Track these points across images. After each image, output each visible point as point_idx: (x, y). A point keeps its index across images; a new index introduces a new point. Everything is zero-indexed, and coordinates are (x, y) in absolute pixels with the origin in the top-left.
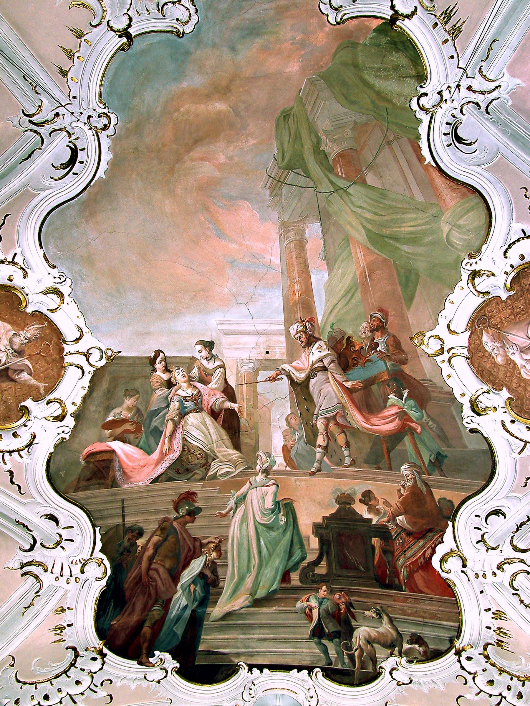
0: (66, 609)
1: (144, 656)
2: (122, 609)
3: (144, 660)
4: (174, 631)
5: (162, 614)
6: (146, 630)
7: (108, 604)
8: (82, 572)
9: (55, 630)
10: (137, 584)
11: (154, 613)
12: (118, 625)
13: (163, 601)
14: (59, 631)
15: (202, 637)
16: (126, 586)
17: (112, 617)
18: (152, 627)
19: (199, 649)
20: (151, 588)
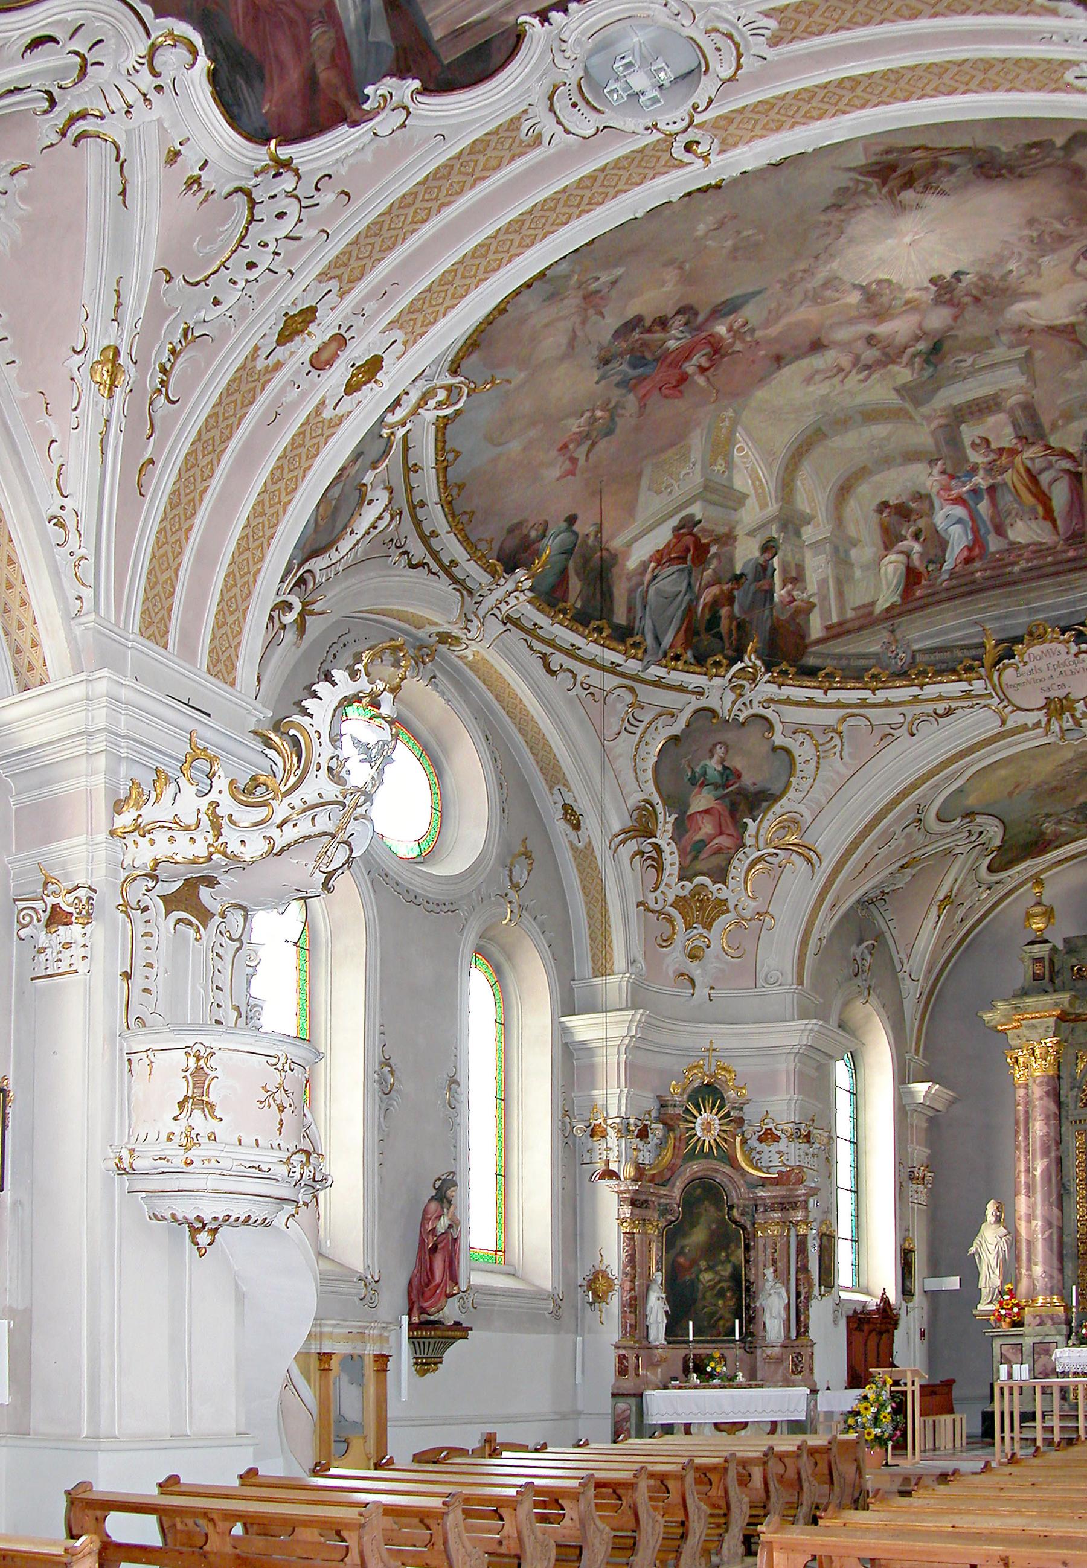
0: (180, 147)
1: (352, 110)
2: (262, 79)
3: (356, 115)
4: (374, 43)
5: (332, 35)
6: (325, 75)
7: (232, 86)
8: (156, 75)
9: (189, 187)
10: (256, 19)
11: (319, 43)
12: (276, 106)
13: (320, 12)
14: (195, 187)
15: (428, 18)
16: (242, 37)
17: (258, 102)
18: (333, 64)
19: (436, 39)
20: (284, 7)
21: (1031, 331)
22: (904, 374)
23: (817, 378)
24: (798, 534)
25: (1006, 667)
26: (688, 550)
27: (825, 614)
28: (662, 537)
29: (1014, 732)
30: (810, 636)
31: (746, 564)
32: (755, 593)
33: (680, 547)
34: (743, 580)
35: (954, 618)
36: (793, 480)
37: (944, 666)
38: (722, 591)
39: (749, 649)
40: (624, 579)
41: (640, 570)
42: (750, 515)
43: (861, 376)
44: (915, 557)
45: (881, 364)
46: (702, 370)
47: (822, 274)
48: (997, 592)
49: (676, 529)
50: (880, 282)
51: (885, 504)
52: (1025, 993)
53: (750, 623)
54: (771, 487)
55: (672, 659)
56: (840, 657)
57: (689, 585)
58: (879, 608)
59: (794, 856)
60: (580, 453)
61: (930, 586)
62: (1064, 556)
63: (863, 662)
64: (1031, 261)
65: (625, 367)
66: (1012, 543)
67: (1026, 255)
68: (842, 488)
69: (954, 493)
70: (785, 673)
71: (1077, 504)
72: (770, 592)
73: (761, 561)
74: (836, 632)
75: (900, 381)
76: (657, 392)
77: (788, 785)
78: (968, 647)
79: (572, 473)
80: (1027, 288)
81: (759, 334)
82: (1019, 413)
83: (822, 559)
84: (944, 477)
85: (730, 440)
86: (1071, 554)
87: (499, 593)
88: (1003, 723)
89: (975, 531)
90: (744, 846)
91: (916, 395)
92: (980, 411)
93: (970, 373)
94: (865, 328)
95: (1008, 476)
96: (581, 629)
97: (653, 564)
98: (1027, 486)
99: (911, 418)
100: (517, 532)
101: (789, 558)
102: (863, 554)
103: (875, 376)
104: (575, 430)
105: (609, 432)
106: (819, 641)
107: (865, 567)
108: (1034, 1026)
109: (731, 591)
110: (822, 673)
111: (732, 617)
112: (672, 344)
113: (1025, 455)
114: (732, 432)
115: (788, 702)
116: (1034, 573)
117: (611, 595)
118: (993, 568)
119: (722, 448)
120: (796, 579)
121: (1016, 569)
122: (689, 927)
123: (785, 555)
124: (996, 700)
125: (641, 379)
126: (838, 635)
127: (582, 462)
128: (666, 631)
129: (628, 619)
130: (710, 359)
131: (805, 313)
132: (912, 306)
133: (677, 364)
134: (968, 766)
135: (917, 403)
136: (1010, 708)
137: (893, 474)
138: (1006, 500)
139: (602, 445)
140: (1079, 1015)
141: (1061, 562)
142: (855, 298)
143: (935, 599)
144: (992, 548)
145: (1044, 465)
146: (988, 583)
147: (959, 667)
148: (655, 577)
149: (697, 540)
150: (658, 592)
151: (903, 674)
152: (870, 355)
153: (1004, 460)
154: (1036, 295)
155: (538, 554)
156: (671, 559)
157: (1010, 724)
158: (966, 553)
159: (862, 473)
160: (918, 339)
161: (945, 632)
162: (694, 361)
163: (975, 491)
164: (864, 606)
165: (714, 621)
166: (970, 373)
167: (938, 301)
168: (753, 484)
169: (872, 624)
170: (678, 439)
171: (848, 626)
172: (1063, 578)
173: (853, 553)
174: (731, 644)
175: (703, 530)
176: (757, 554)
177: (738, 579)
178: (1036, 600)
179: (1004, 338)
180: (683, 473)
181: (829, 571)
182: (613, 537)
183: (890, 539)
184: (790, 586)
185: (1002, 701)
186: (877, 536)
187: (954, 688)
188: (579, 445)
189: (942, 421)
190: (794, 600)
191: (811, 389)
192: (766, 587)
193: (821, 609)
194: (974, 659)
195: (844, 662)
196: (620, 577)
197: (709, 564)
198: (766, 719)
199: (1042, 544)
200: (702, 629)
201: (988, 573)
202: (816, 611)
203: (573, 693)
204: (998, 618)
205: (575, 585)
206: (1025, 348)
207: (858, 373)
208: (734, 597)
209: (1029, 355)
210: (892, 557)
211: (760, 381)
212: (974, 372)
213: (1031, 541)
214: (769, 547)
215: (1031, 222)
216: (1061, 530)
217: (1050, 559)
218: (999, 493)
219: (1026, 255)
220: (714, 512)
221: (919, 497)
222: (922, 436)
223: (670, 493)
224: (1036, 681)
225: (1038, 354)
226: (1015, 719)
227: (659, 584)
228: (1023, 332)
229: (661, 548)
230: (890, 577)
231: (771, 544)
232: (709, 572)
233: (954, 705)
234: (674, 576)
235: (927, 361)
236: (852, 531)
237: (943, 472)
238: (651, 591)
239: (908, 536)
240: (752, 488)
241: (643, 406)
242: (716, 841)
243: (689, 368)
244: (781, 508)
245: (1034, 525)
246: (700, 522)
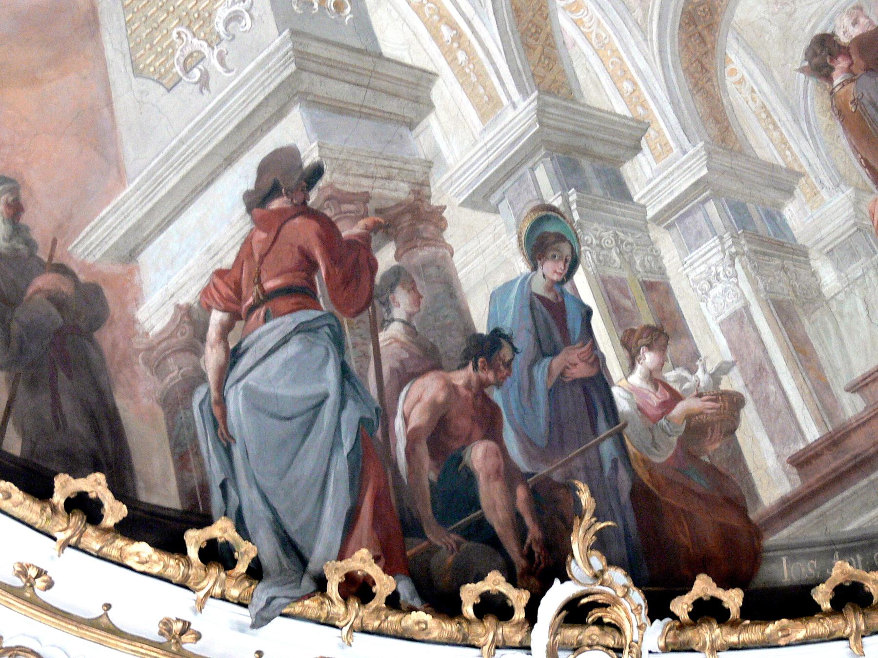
30: (756, 498)
31: (497, 297)
32: (553, 393)
34: (506, 352)
38: (452, 388)
39: (575, 547)
40: (141, 368)
41: (181, 339)
57: (345, 373)
73: (539, 286)
97: (217, 317)
109: (480, 390)
123: (603, 262)
148: (234, 356)
156: (268, 297)
168: (436, 37)
175: (338, 198)
176: (521, 267)
180: (222, 14)
181: (746, 287)
184: (649, 358)
190: (676, 397)
192: (581, 371)
193: (763, 404)
196: (126, 361)
197: (387, 304)
200: (426, 511)
202: (749, 415)
208: (495, 409)
223: (204, 83)
229: (228, 261)
231: (551, 228)
232: (395, 330)
234: (292, 348)
238: (235, 400)
240: (433, 49)
244: (541, 111)
246: (317, 172)
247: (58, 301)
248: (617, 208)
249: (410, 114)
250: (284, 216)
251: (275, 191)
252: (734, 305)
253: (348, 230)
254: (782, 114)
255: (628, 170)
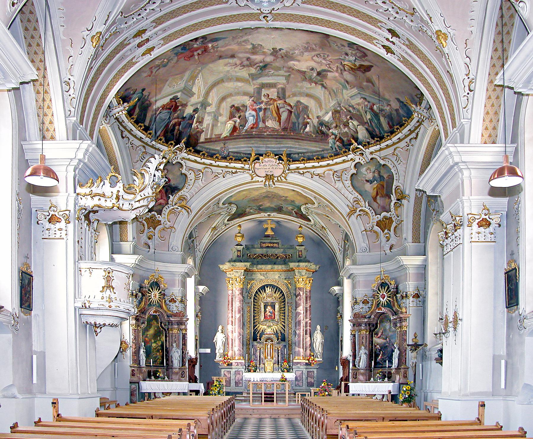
21: (293, 69)
22: (253, 70)
23: (229, 65)
24: (205, 109)
25: (257, 162)
26: (172, 106)
27: (206, 134)
28: (166, 100)
29: (254, 182)
31: (187, 114)
33: (171, 105)
35: (244, 144)
36: (209, 92)
37: (237, 158)
42: (194, 100)
43: (241, 68)
44: (237, 124)
45: (248, 66)
46: (199, 54)
47: (245, 38)
48: (258, 139)
49: (171, 99)
50: (259, 45)
51: (233, 106)
52: (235, 261)
53: (183, 132)
54: (203, 92)
55: (159, 140)
56: (207, 149)
57: (170, 117)
58: (222, 137)
59: (183, 210)
60: (154, 72)
61: (238, 133)
62: (280, 133)
63: (213, 152)
64: (302, 52)
65: (180, 49)
66: (266, 126)
67: (301, 50)
68: (223, 98)
69: (254, 108)
70: (190, 151)
71: (288, 120)
72: (192, 124)
74: (208, 141)
75: (251, 72)
76: (183, 58)
77: (184, 186)
78: (245, 154)
79: (150, 76)
80: (297, 58)
81: (219, 49)
82: (280, 90)
83: (210, 118)
84: (253, 102)
85: (196, 77)
86: (282, 133)
87: (118, 110)
88: (252, 179)
89: (257, 120)
90: (168, 204)
91: (253, 77)
92: (270, 86)
93: (271, 75)
94: (248, 55)
95: (271, 107)
96: (136, 125)
97: (161, 108)
98: (276, 111)
99: (250, 83)
100: (128, 91)
101: (200, 115)
102: (222, 119)
103: (245, 69)
104: (157, 63)
105: (165, 66)
106: (202, 143)
107: (222, 123)
108: (237, 272)
109: (181, 122)
110: (201, 153)
111: (179, 130)
112: (195, 46)
113: (278, 102)
114: (198, 74)
115: (189, 160)
116: (271, 137)
117: (146, 116)
118: (258, 132)
119: (193, 78)
120: (200, 122)
121: (265, 134)
122: (149, 228)
124: (251, 172)
125: (182, 53)
126: (208, 142)
127: (153, 74)
128: (159, 131)
129: (149, 125)
130: (202, 53)
131: (234, 47)
132: (264, 53)
133: (193, 52)
134: (236, 190)
135: (253, 79)
136: (255, 175)
137: (238, 97)
138: (268, 113)
139: (161, 69)
140: (250, 270)
141: (278, 135)
142: (250, 47)
143: (239, 137)
144: (260, 126)
145: (283, 106)
146: (257, 136)
147: (242, 160)
148: (160, 113)
149: (176, 103)
150: (160, 118)
151: (224, 158)
152: (246, 63)
153: (272, 102)
154: (299, 61)
155: (130, 99)
156: (167, 108)
157: (254, 180)
158: (252, 126)
159: (230, 95)
160: (261, 62)
161: (240, 148)
162: (198, 52)
163: (260, 109)
164: (219, 135)
165: (173, 130)
166: (271, 75)
167: (272, 54)
169: (219, 141)
170: (183, 72)
171: (212, 140)
172: (278, 140)
173: (219, 118)
174: (176, 138)
175: (179, 101)
176: (192, 112)
177: (184, 118)
178: (269, 144)
179: (285, 69)
182: (152, 98)
183: (232, 116)
184: (198, 124)
185: (253, 172)
186: (228, 114)
187: (239, 165)
188: (155, 68)
189: (258, 86)
191: (225, 68)
192: (191, 123)
194: (247, 158)
195: (208, 150)
198: (182, 164)
199: (274, 128)
201: (257, 133)
202: (204, 133)
203: (127, 145)
204: (256, 147)
205: (137, 110)
206: (289, 73)
207: (241, 67)
209: (290, 75)
210: (230, 122)
211: (213, 61)
212: (272, 75)
213: (272, 127)
214: (196, 111)
215: (308, 43)
216: (281, 126)
217: (276, 133)
218: (267, 110)
219: (301, 50)
220: (184, 97)
221: (244, 106)
222: (251, 89)
224: (264, 169)
225: (292, 76)
226: (256, 179)
227: (161, 115)
228: (291, 69)
230: (228, 127)
233: (238, 171)
235: (261, 69)
236: (221, 111)
237: (253, 101)
239: (237, 117)
241: (177, 61)
242: (160, 201)
243: (195, 53)
245: (274, 122)
246: (179, 98)
247: (147, 104)
248: (204, 110)
249: (191, 96)
250: (173, 101)
251: (173, 99)
252: (209, 123)
253: (178, 105)
254: (225, 109)
255: (207, 108)
